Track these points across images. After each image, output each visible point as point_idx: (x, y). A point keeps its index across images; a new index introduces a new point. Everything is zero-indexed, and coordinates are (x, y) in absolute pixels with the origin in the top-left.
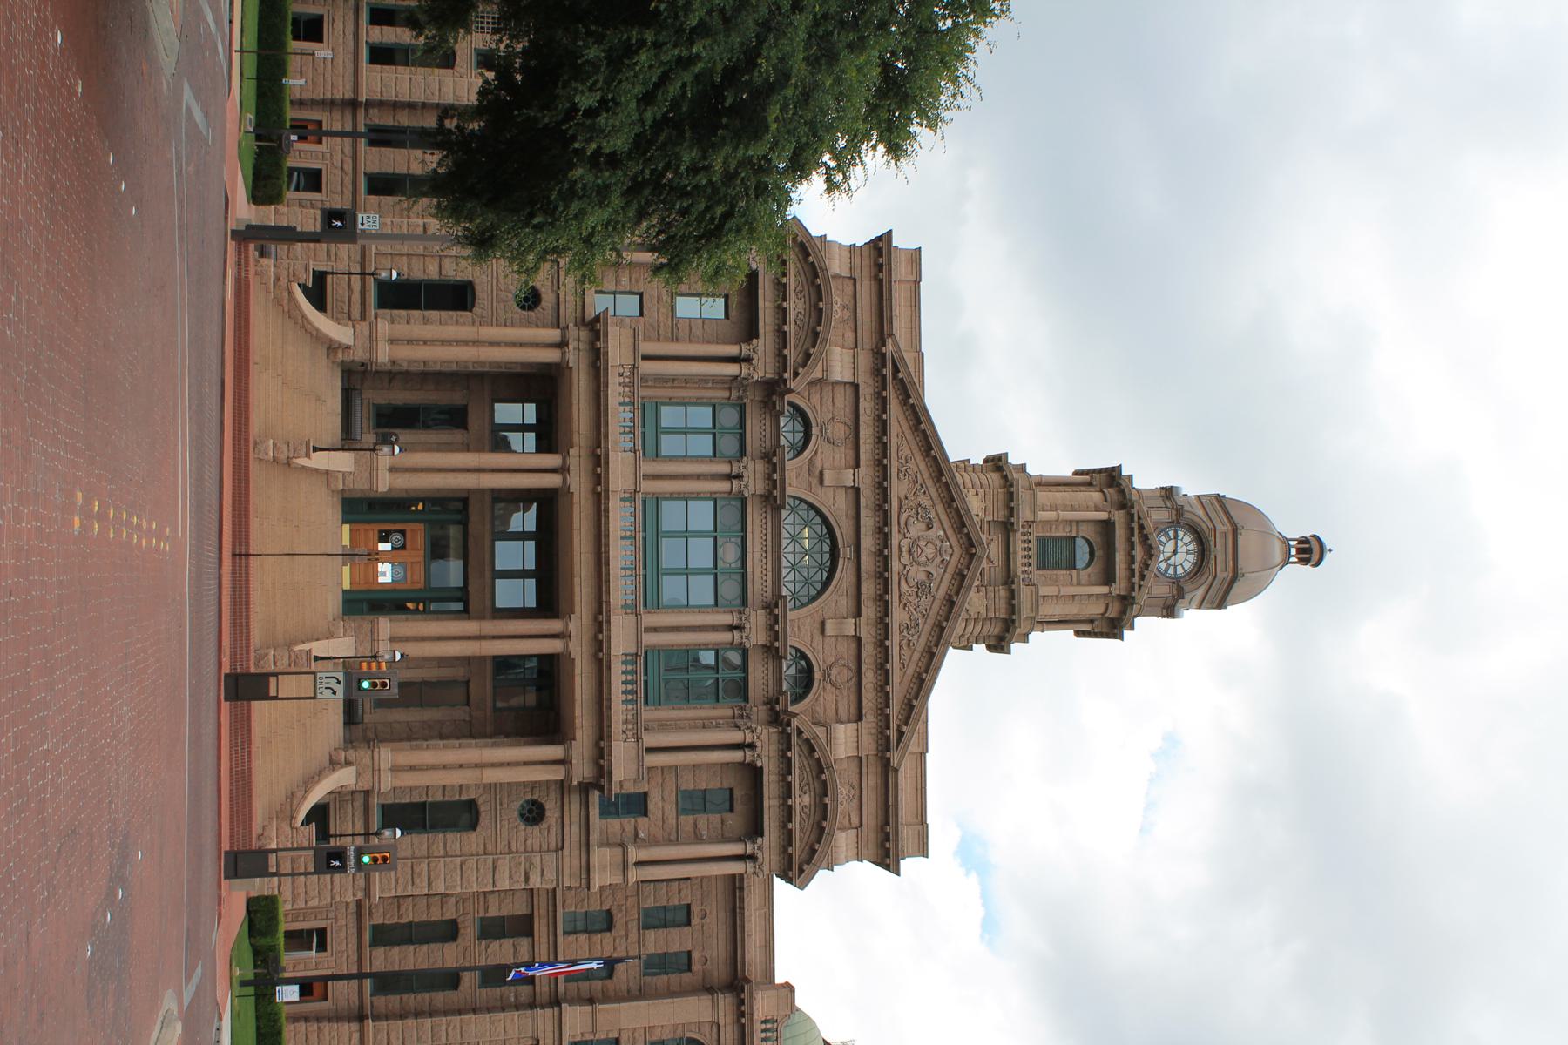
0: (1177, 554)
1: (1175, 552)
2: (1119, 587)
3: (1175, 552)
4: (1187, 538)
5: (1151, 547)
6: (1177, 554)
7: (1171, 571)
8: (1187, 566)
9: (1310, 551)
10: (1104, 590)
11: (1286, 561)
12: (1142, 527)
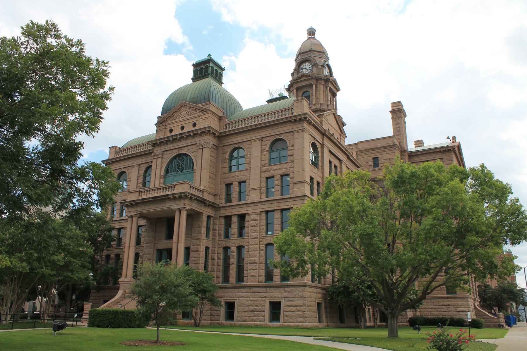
0: (306, 68)
1: (306, 69)
2: (314, 82)
3: (306, 69)
4: (302, 66)
5: (302, 76)
6: (306, 68)
9: (311, 32)
10: (314, 86)
11: (314, 38)
12: (297, 79)
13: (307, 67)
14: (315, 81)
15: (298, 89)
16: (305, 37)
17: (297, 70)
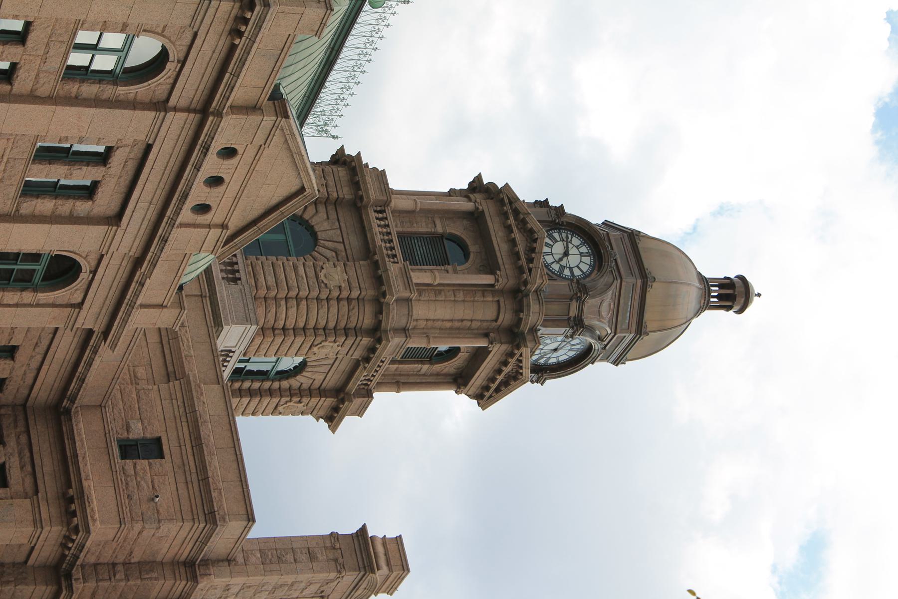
1: (566, 254)
3: (566, 254)
4: (576, 241)
5: (532, 231)
7: (567, 272)
8: (585, 268)
9: (733, 294)
10: (487, 279)
13: (573, 260)
14: (511, 283)
15: (475, 218)
16: (715, 267)
17: (559, 220)
